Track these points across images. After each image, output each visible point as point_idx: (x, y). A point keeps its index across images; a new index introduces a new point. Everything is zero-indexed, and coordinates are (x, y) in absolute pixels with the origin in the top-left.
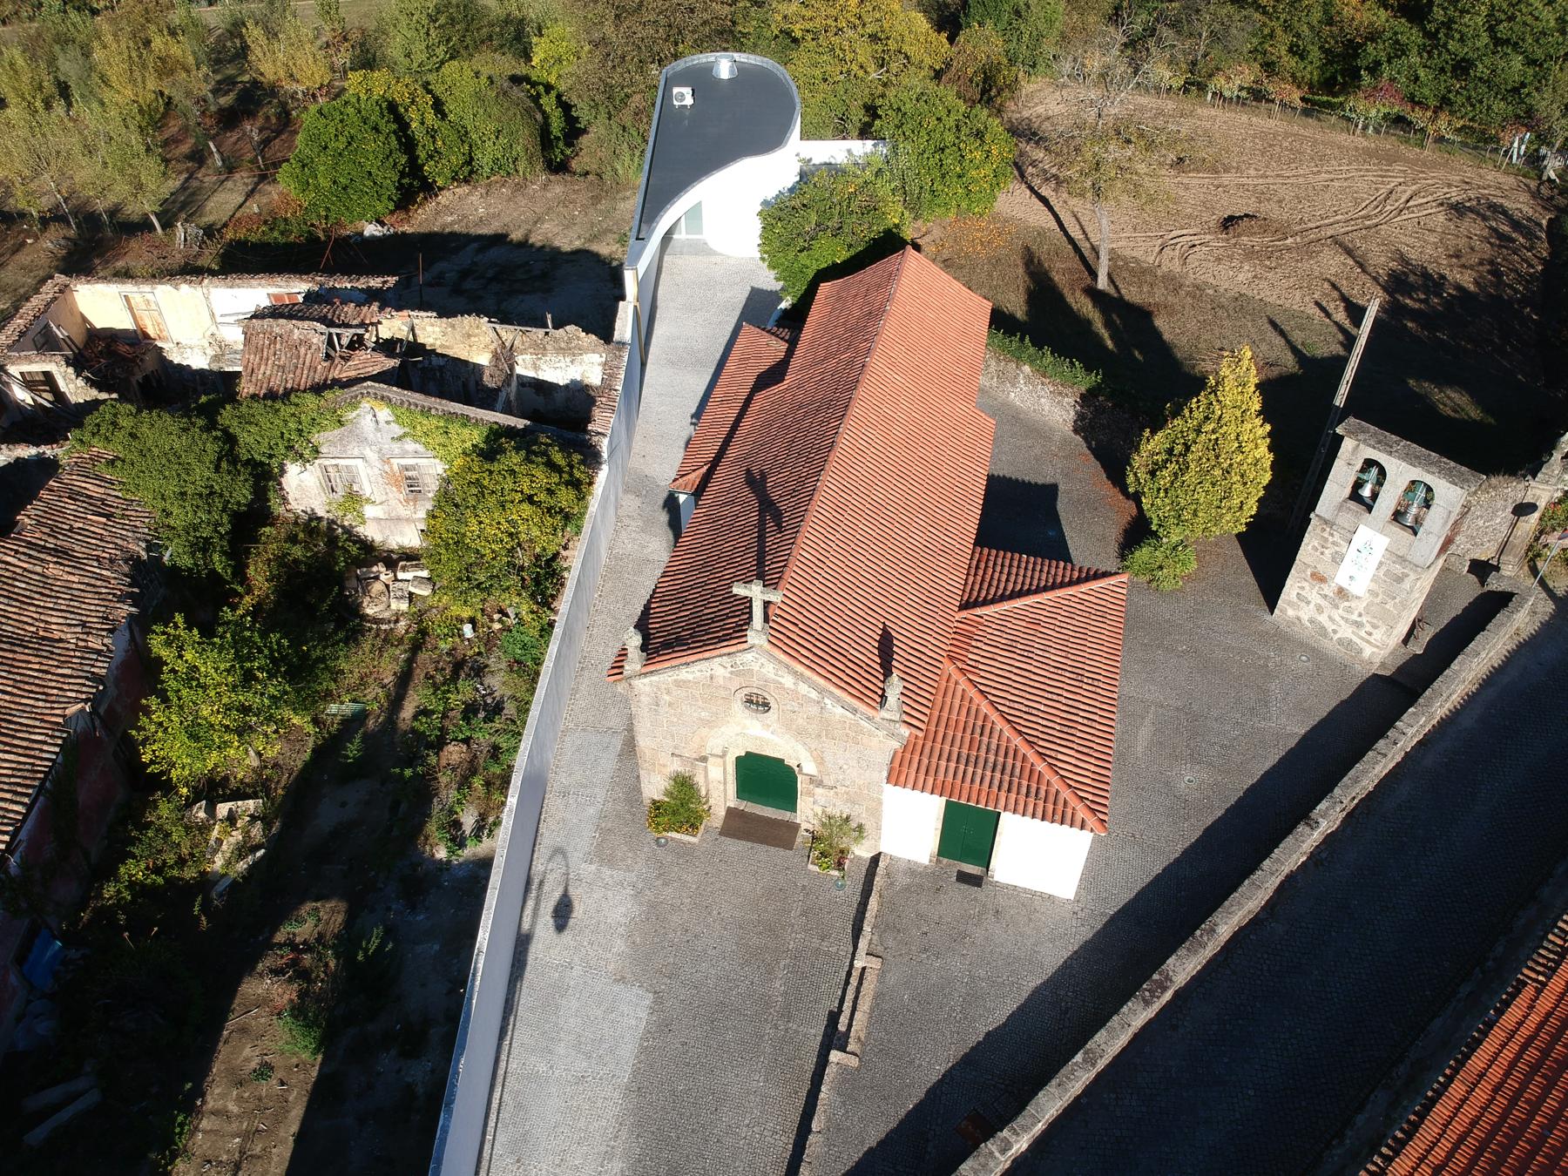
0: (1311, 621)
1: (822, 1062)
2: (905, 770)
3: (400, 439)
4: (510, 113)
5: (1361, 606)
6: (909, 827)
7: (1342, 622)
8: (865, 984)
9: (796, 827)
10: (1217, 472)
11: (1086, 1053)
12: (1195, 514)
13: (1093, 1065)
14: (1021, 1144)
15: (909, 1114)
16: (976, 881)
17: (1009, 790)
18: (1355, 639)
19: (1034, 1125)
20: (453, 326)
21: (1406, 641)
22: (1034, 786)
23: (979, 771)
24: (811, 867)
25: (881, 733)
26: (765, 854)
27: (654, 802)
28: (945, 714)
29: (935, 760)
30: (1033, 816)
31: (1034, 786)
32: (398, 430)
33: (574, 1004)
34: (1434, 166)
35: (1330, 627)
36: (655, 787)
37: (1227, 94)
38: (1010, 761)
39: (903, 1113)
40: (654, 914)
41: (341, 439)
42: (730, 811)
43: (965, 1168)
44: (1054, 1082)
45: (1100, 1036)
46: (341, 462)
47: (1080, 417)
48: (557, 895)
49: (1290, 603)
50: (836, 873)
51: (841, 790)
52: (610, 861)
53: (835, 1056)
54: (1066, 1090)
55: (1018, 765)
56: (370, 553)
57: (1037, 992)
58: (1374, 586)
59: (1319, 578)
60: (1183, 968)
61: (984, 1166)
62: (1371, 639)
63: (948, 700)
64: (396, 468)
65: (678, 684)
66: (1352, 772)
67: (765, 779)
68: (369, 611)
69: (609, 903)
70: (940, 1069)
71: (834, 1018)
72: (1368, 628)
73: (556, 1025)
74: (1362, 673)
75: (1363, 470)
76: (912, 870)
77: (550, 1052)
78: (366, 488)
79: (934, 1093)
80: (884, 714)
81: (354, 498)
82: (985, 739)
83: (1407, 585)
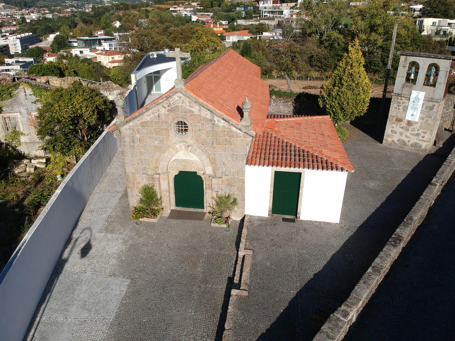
0: (399, 141)
1: (228, 295)
2: (254, 159)
3: (35, 102)
4: (100, 76)
5: (418, 126)
6: (257, 195)
7: (411, 136)
8: (246, 261)
9: (205, 213)
10: (354, 85)
11: (373, 268)
12: (348, 103)
13: (379, 272)
14: (353, 315)
15: (281, 314)
16: (293, 221)
17: (304, 161)
18: (418, 142)
19: (358, 302)
20: (64, 81)
21: (435, 144)
22: (315, 159)
23: (289, 157)
24: (212, 224)
25: (242, 134)
26: (189, 223)
27: (135, 208)
28: (269, 143)
29: (267, 155)
30: (318, 169)
31: (315, 159)
32: (34, 98)
33: (84, 288)
34: (376, 87)
35: (406, 140)
36: (135, 199)
37: (314, 76)
38: (301, 153)
39: (278, 314)
40: (133, 249)
41: (11, 104)
42: (172, 211)
43: (325, 327)
44: (361, 281)
45: (377, 260)
46: (10, 114)
47: (295, 108)
48: (82, 245)
49: (389, 136)
50: (225, 226)
51: (225, 178)
52: (112, 232)
53: (234, 292)
54: (369, 285)
55: (306, 154)
56: (21, 157)
57: (334, 256)
58: (422, 115)
59: (399, 120)
60: (406, 232)
61: (336, 325)
62: (425, 139)
63: (269, 139)
64: (33, 117)
65: (144, 124)
66: (440, 171)
67: (189, 187)
68: (16, 172)
69: (110, 246)
70: (293, 293)
71: (231, 280)
72: (422, 135)
73: (72, 298)
74: (423, 155)
75: (410, 69)
76: (261, 219)
77: (67, 311)
78: (21, 128)
79: (293, 303)
80: (243, 123)
81: (16, 134)
82: (288, 148)
83: (435, 110)
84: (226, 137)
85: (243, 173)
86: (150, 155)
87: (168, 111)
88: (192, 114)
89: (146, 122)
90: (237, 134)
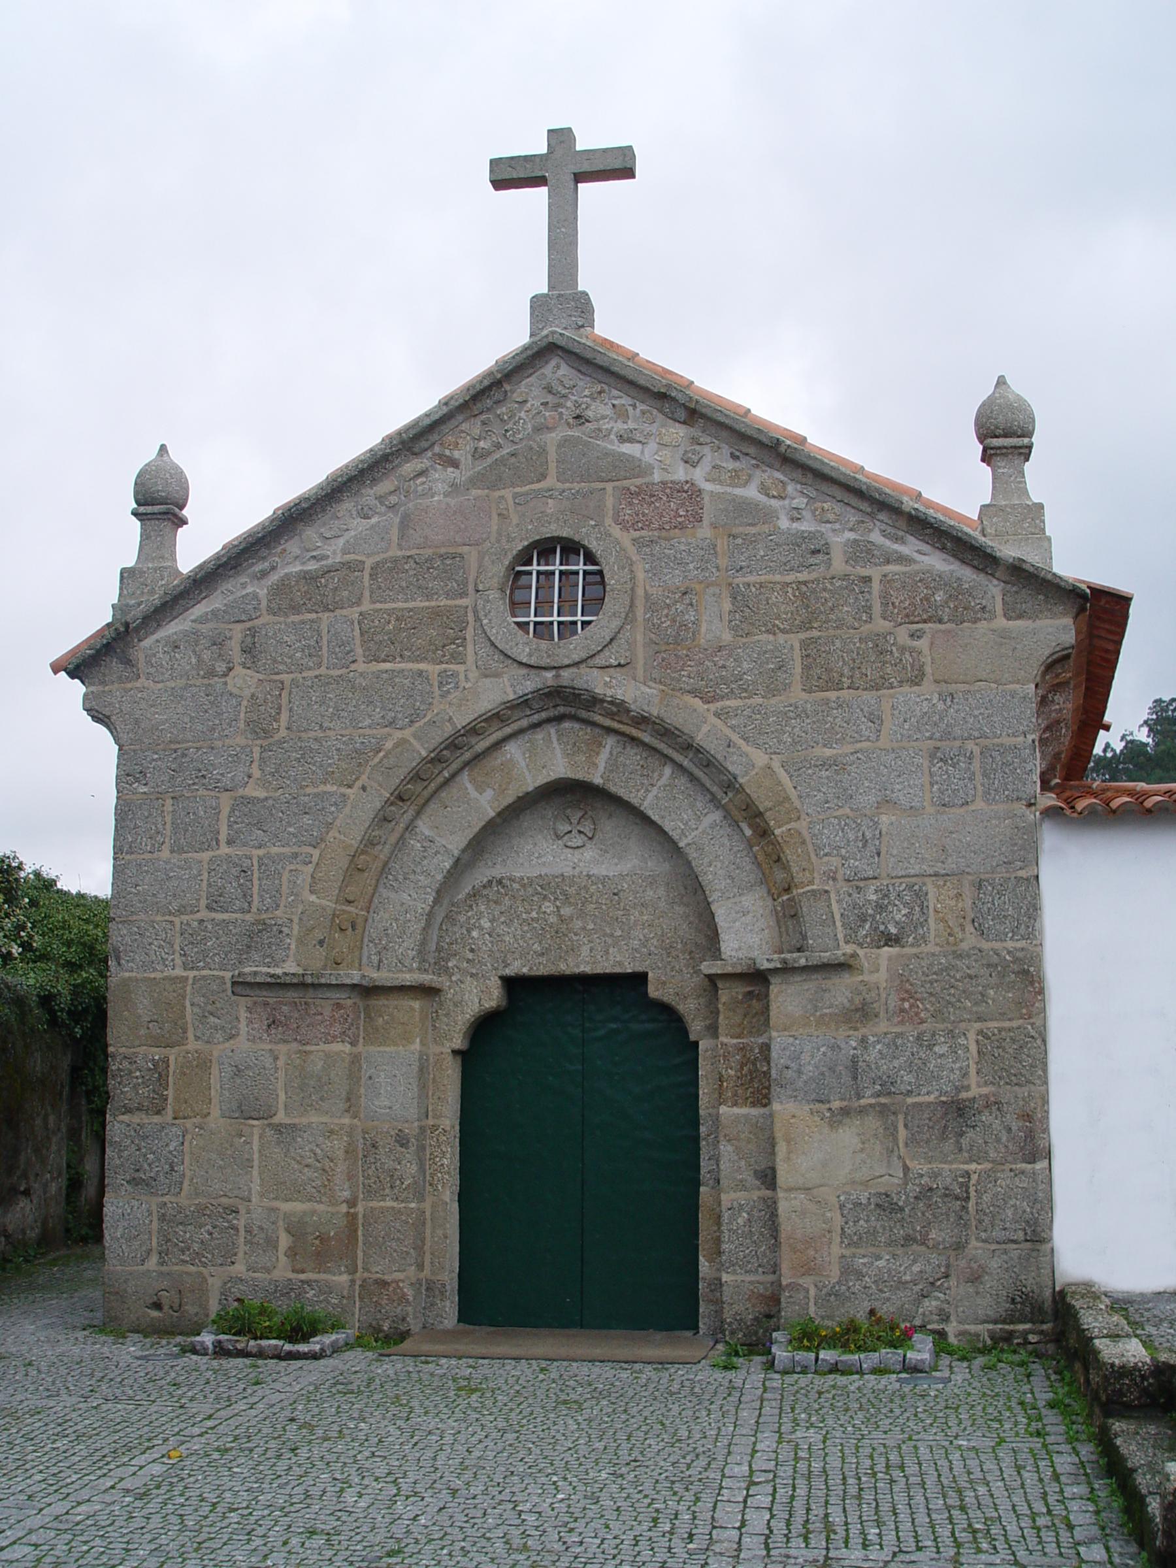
84: (881, 625)
85: (1014, 902)
86: (307, 820)
87: (473, 482)
88: (633, 484)
89: (309, 578)
90: (956, 592)
